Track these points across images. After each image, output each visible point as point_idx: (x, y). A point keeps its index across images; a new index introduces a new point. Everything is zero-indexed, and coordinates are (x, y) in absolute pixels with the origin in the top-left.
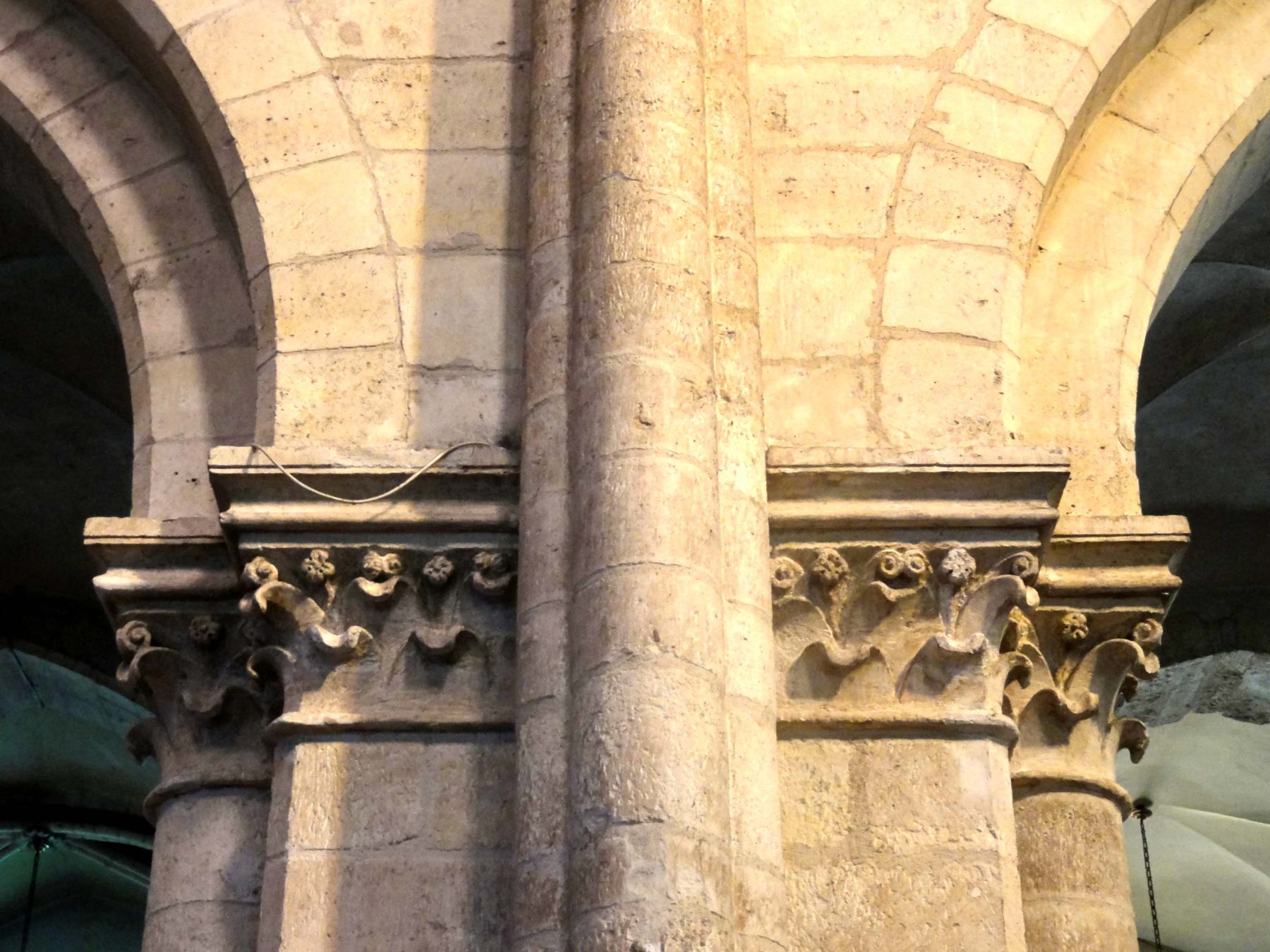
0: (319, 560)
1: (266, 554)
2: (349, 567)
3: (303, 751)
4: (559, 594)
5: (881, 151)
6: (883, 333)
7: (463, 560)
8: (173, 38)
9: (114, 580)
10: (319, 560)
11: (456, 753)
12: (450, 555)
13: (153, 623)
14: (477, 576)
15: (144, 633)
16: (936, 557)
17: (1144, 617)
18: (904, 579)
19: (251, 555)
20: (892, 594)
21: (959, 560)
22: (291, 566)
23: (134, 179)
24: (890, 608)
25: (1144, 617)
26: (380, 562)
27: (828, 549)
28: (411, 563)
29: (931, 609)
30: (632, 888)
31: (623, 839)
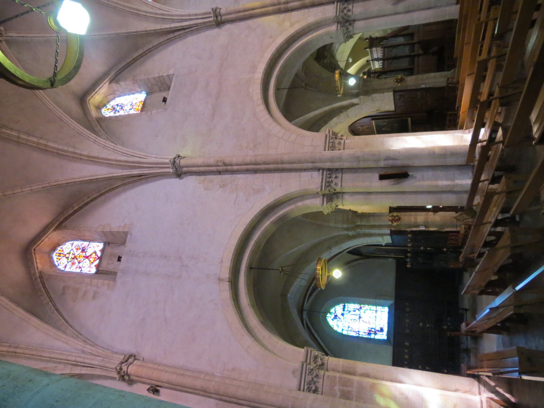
0: (328, 184)
2: (328, 182)
6: (312, 145)
10: (328, 184)
14: (330, 173)
16: (331, 142)
18: (333, 145)
20: (334, 145)
21: (332, 141)
23: (285, 207)
24: (334, 146)
26: (328, 180)
27: (330, 149)
28: (329, 178)
29: (335, 144)
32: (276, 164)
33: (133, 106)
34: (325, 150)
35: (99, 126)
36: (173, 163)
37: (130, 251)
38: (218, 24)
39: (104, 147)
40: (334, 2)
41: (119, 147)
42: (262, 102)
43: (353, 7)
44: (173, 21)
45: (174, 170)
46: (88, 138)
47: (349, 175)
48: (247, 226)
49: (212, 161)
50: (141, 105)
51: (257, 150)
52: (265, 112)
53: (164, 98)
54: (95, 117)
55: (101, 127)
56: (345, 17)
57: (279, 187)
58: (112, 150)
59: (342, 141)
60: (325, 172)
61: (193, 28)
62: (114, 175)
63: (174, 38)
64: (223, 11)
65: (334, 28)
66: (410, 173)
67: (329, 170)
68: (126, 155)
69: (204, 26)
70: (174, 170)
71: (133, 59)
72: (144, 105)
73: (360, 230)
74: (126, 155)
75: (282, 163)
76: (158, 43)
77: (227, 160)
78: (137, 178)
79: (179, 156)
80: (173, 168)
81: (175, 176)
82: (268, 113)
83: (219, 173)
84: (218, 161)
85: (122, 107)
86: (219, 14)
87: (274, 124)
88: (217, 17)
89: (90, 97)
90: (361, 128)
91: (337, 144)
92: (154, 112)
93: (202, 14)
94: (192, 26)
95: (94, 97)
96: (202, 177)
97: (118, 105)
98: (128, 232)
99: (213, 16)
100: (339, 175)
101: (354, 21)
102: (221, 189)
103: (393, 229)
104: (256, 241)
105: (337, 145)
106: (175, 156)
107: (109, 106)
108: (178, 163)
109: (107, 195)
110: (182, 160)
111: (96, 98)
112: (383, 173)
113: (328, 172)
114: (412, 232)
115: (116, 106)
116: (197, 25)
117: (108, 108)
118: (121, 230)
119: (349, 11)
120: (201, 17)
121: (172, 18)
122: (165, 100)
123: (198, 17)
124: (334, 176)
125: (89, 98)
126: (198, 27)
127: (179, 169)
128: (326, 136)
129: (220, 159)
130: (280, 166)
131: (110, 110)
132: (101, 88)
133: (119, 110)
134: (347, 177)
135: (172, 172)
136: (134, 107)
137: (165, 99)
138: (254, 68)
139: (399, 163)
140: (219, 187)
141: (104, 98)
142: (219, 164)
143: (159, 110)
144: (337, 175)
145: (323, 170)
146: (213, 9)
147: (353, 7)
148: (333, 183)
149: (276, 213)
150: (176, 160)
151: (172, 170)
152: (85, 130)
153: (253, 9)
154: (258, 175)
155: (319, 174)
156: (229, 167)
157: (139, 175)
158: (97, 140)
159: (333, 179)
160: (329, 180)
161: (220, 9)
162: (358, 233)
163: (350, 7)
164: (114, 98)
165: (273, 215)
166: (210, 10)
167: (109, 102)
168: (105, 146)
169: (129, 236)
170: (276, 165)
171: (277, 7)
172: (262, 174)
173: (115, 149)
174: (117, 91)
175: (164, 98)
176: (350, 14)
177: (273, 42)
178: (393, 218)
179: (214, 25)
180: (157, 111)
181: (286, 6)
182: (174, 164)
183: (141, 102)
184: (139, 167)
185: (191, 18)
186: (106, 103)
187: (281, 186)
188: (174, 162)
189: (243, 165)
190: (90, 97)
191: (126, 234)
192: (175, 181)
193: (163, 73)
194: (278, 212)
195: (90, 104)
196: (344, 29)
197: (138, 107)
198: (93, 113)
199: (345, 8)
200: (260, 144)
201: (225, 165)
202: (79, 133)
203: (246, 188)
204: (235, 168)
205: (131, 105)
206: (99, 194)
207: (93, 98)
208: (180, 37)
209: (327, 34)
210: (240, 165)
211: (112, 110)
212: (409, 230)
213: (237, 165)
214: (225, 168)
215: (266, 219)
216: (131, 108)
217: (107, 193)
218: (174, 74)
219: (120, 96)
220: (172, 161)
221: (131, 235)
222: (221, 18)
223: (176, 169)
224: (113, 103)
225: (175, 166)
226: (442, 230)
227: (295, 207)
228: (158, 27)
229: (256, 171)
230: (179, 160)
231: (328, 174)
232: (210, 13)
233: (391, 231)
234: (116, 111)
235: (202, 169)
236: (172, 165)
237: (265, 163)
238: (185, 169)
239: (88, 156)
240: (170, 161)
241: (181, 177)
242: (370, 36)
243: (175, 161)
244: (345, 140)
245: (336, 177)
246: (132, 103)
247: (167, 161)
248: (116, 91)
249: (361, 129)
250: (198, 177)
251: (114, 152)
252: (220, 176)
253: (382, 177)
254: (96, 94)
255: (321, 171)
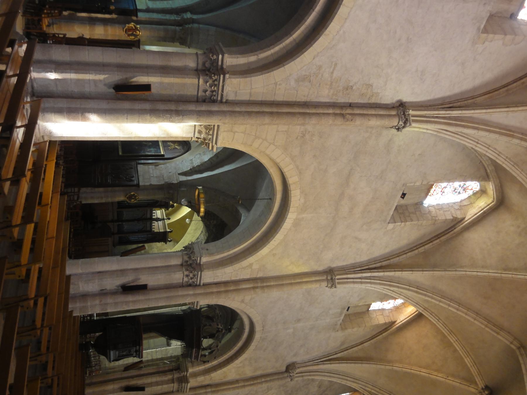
0: (216, 83)
1: (217, 78)
2: (215, 85)
3: (197, 80)
4: (206, 109)
5: (256, 134)
6: (234, 133)
7: (215, 96)
8: (284, 66)
9: (220, 56)
10: (216, 83)
11: (196, 93)
12: (215, 94)
13: (216, 59)
14: (213, 97)
15: (214, 58)
17: (207, 146)
19: (217, 76)
20: (208, 131)
22: (216, 80)
23: (272, 55)
24: (207, 130)
25: (207, 146)
26: (215, 88)
27: (212, 127)
28: (215, 91)
29: (206, 133)
30: (177, 118)
31: (181, 117)
32: (280, 112)
33: (441, 191)
34: (218, 126)
35: (488, 171)
36: (406, 122)
37: (485, 4)
38: (331, 271)
39: (489, 146)
40: (203, 285)
41: (469, 144)
42: (290, 186)
43: (183, 278)
44: (379, 278)
45: (408, 113)
46: (507, 159)
47: (189, 93)
48: (323, 32)
49: (359, 121)
50: (432, 191)
51: (302, 131)
52: (287, 174)
53: (403, 198)
54: (490, 183)
55: (486, 170)
56: (192, 269)
57: (278, 83)
58: (479, 142)
59: (197, 135)
60: (219, 98)
61: (360, 269)
62: (484, 111)
63: (381, 261)
64: (324, 284)
65: (204, 260)
66: (112, 90)
67: (214, 102)
68: (463, 135)
69: (347, 271)
70: (407, 112)
71: (432, 242)
72: (429, 191)
73: (176, 18)
74: (463, 135)
75: (271, 113)
76: (401, 257)
77: (339, 121)
78: (455, 105)
79: (398, 129)
80: (409, 115)
81: (406, 105)
82: (284, 174)
83: (351, 106)
84: (351, 120)
85: (454, 191)
86: (329, 282)
87: (278, 161)
88: (332, 279)
89: (490, 205)
90: (177, 147)
91: (203, 132)
92: (418, 184)
93: (347, 283)
94: (360, 271)
95: (486, 205)
96: (373, 101)
97: (459, 193)
98: (482, 33)
99: (336, 280)
100: (201, 94)
101: (182, 265)
102: (351, 84)
103: (134, 18)
104: (313, 10)
105: (204, 130)
106: (405, 130)
107: (470, 193)
108: (400, 121)
109: (498, 85)
110: (396, 124)
111: (483, 203)
112: (147, 93)
113: (215, 98)
114: (110, 13)
115: (461, 192)
116: (355, 272)
117: (472, 191)
118: (491, 36)
119: (187, 276)
120: (349, 280)
121: (381, 282)
122: (404, 195)
123: (352, 280)
124: (208, 93)
125: (493, 203)
126: (354, 270)
127: (400, 113)
128: (216, 143)
129: (347, 123)
130: (275, 110)
131: (470, 188)
132: (476, 214)
133: (459, 187)
134: (191, 92)
135: (411, 111)
136: (440, 190)
137: (403, 196)
138: (297, 223)
139: (127, 105)
140: (354, 88)
141: (474, 203)
142: (350, 117)
143: (412, 184)
144: (204, 94)
145: (221, 102)
146: (335, 287)
147: (183, 278)
148: (210, 85)
149: (284, 47)
150: (403, 125)
151: (409, 113)
152: (508, 169)
153: (291, 284)
154: (303, 100)
155: (227, 96)
156: (338, 111)
157: (452, 109)
158: (496, 156)
159: (209, 90)
160: (214, 88)
161: (326, 287)
162: (180, 15)
163: (186, 279)
164: (461, 201)
165: (287, 45)
166: (338, 286)
167: (469, 197)
168: (488, 148)
169: (482, 26)
170: (280, 111)
171: (265, 284)
172: (298, 100)
173: (475, 144)
174: (456, 209)
175: (403, 198)
176: (186, 273)
177: (272, 250)
178: (135, 33)
179: (335, 271)
180: (415, 185)
181: (256, 285)
182: (407, 120)
183: (431, 195)
184: (450, 118)
185: (360, 280)
186: (472, 197)
187: (276, 84)
188: (405, 123)
189: (320, 113)
190: (490, 205)
191: (485, 31)
192: (407, 98)
193: (400, 225)
194: (281, 49)
195: (493, 197)
196: (193, 257)
197: (436, 189)
198: (491, 187)
199: (192, 278)
200: (297, 138)
201: (343, 115)
202: (517, 165)
203: (320, 84)
204: (331, 111)
205: (444, 192)
206: (509, 87)
207: (488, 204)
208: (375, 260)
209: (212, 254)
210: (324, 114)
211: (467, 188)
212: (114, 16)
213: (329, 114)
214: (344, 112)
215: (297, 41)
216: (444, 189)
217: (498, 88)
218: (389, 223)
219: (454, 203)
220: (408, 125)
221: (479, 29)
222: (327, 278)
223: (404, 114)
224: (464, 196)
225: (405, 117)
226: (71, 12)
227: (259, 55)
228: (398, 274)
229: (305, 104)
230: (399, 124)
231: (215, 96)
232: (339, 283)
233: (137, 16)
234: (463, 186)
235: (372, 112)
236: (408, 119)
237: (293, 114)
238: (394, 113)
239: (513, 136)
240: (410, 125)
241: (400, 103)
242: (166, 244)
243: (404, 124)
244: (194, 136)
245: (205, 91)
246: (442, 194)
247: (414, 125)
248: (458, 209)
249: (176, 146)
250: (378, 101)
251: (478, 140)
252: (350, 101)
253: (147, 87)
254: (482, 208)
255: (224, 100)
